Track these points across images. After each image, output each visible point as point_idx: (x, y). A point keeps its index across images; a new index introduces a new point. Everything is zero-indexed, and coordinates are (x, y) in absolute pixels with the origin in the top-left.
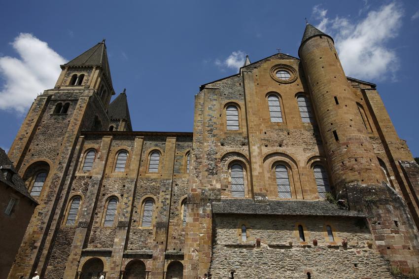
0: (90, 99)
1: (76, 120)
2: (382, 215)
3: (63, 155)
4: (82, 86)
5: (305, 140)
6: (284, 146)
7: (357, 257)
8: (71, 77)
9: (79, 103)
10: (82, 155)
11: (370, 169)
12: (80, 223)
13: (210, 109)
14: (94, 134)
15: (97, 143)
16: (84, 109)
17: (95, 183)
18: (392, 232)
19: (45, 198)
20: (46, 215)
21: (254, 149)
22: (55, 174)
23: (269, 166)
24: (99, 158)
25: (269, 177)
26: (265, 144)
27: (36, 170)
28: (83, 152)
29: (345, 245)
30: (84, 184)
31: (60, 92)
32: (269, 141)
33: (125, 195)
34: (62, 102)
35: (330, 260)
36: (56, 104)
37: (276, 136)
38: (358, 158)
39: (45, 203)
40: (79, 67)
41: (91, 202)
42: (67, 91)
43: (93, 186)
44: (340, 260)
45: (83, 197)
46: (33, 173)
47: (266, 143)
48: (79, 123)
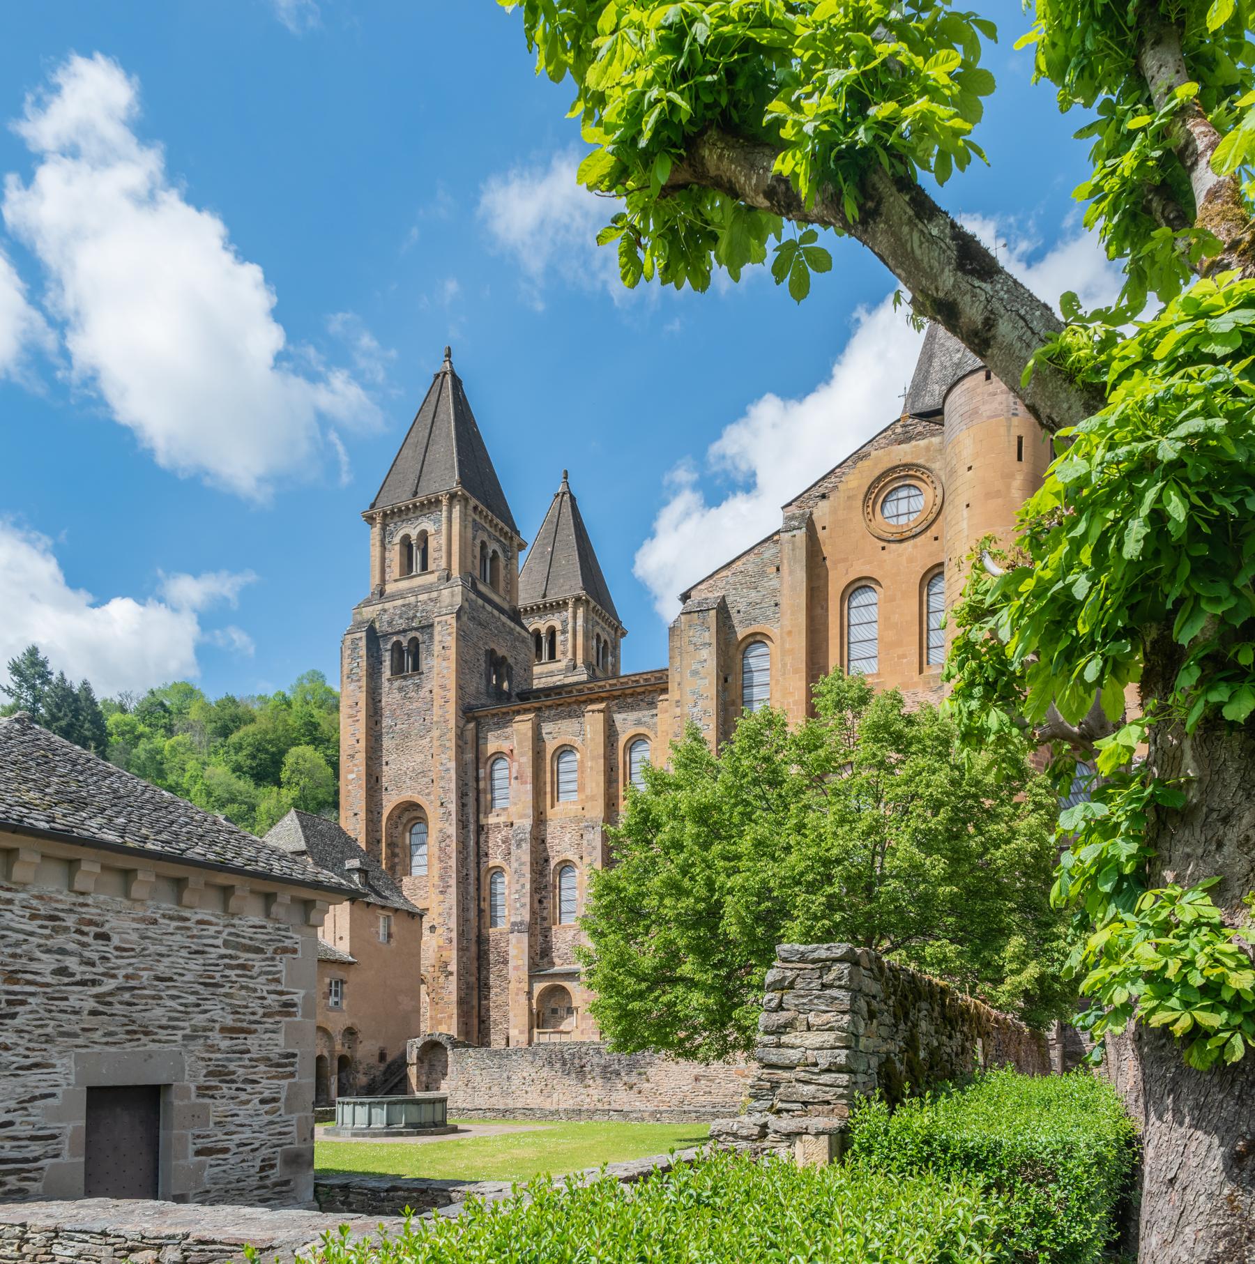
0: (458, 618)
1: (442, 687)
3: (442, 784)
4: (432, 572)
8: (397, 548)
9: (437, 638)
10: (482, 771)
12: (514, 924)
14: (494, 715)
15: (507, 738)
16: (452, 653)
17: (521, 840)
19: (436, 880)
20: (450, 915)
22: (441, 831)
24: (516, 778)
27: (404, 820)
28: (481, 765)
30: (504, 842)
31: (387, 606)
33: (587, 860)
34: (401, 638)
36: (389, 647)
39: (441, 892)
40: (408, 508)
41: (522, 881)
42: (400, 602)
43: (519, 846)
45: (507, 868)
46: (400, 828)
48: (452, 695)
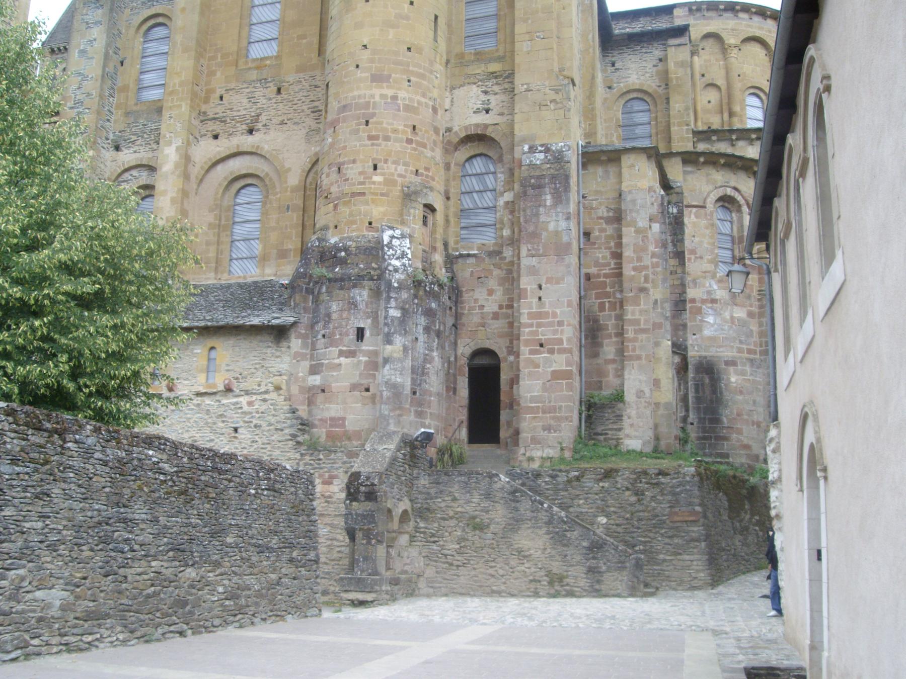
2: (334, 316)
5: (316, 104)
6: (258, 130)
7: (242, 413)
11: (363, 194)
13: (83, 52)
18: (341, 354)
21: (168, 155)
23: (217, 193)
25: (210, 224)
26: (213, 131)
29: (228, 390)
32: (225, 121)
35: (192, 421)
37: (245, 101)
38: (343, 163)
44: (209, 421)
47: (216, 127)
